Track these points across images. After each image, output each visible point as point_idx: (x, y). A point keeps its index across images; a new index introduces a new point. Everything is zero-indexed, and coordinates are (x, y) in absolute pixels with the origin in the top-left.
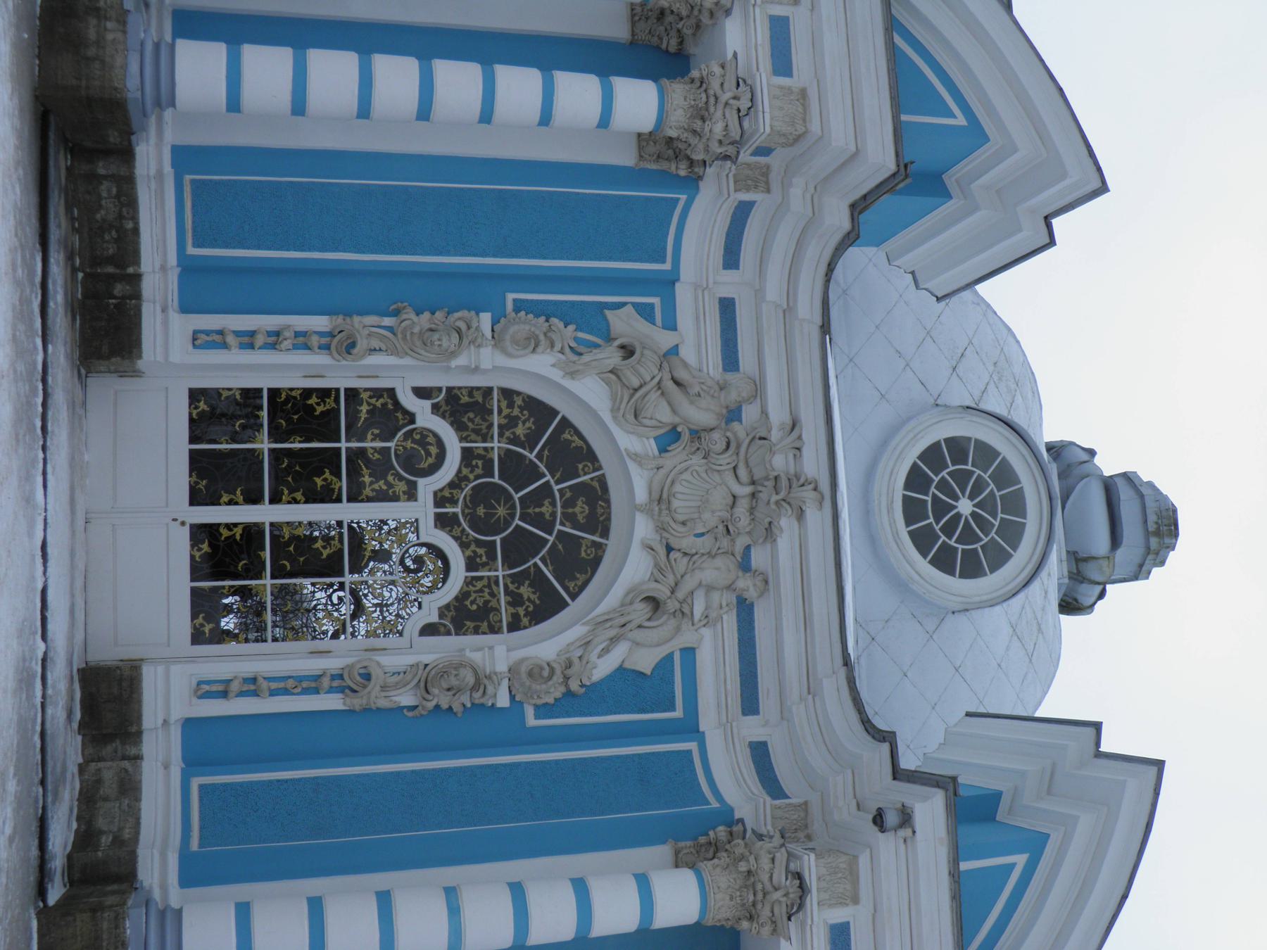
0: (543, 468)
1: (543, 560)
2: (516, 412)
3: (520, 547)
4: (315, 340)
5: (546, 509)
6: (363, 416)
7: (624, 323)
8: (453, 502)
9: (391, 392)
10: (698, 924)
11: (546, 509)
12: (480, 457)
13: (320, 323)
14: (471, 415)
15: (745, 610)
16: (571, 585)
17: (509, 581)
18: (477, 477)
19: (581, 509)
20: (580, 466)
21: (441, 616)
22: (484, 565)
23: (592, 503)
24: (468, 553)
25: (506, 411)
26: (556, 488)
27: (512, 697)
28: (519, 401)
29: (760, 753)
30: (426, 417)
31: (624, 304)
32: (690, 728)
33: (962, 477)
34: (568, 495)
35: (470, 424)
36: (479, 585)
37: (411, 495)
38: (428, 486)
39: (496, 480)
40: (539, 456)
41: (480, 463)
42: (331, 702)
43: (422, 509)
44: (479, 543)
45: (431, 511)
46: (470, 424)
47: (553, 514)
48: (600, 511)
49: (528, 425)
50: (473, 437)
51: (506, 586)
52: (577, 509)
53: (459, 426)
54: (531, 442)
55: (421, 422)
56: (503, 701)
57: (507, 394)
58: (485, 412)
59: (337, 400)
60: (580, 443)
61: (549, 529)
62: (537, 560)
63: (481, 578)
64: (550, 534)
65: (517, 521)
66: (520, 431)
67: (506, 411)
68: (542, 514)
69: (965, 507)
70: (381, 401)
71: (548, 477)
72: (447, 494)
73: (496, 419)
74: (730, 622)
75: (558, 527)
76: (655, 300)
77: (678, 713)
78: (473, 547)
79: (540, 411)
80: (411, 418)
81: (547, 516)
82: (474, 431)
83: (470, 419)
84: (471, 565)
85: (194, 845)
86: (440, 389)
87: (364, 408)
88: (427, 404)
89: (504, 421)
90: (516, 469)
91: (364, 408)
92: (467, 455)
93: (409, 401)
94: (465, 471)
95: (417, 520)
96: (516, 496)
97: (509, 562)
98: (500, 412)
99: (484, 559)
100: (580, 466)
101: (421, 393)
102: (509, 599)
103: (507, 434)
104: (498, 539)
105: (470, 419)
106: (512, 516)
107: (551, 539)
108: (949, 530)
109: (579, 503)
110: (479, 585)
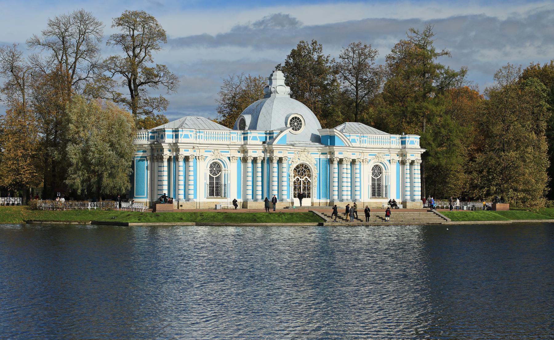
3: (305, 172)
7: (290, 163)
13: (290, 187)
15: (312, 153)
19: (301, 166)
29: (322, 154)
33: (296, 127)
37: (301, 181)
38: (300, 179)
42: (316, 188)
43: (302, 180)
54: (296, 170)
69: (296, 124)
74: (312, 155)
77: (318, 160)
79: (295, 169)
84: (305, 176)
108: (298, 126)
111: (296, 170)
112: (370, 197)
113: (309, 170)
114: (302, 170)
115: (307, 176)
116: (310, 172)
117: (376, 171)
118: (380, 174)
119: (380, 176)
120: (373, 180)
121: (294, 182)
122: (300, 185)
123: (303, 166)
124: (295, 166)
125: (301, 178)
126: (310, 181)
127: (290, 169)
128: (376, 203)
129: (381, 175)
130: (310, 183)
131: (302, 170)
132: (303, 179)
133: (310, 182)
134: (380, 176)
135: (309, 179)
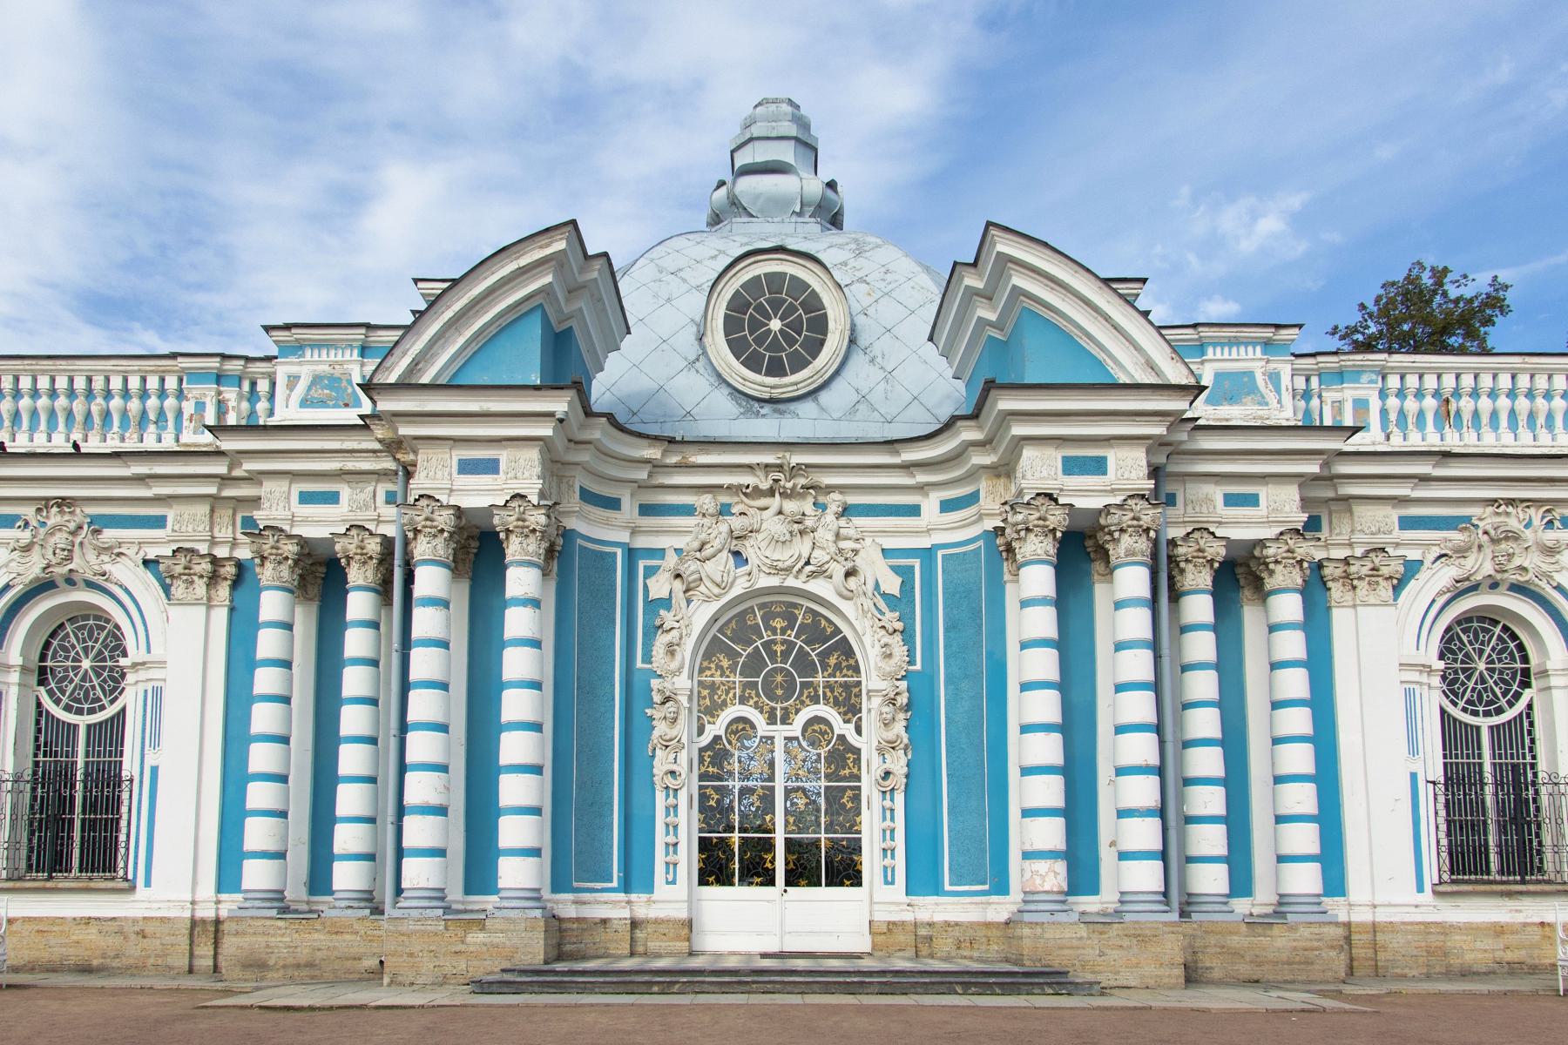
0: (750, 650)
1: (813, 650)
2: (713, 666)
4: (671, 800)
5: (779, 648)
6: (715, 770)
8: (773, 709)
9: (701, 750)
10: (1055, 567)
11: (779, 648)
12: (744, 691)
14: (716, 697)
16: (829, 630)
17: (826, 674)
18: (758, 695)
19: (778, 623)
20: (749, 623)
21: (847, 721)
22: (816, 691)
23: (774, 616)
24: (808, 702)
25: (713, 671)
26: (766, 638)
27: (904, 677)
28: (705, 664)
30: (717, 728)
31: (646, 586)
32: (927, 554)
34: (769, 633)
35: (723, 697)
36: (829, 694)
39: (760, 680)
40: (745, 651)
41: (748, 691)
42: (900, 798)
43: (780, 732)
44: (801, 693)
45: (779, 727)
46: (723, 697)
47: (784, 642)
48: (778, 609)
49: (721, 658)
50: (731, 695)
51: (830, 676)
52: (778, 626)
53: (724, 704)
54: (732, 655)
55: (722, 732)
56: (903, 685)
57: (701, 671)
58: (713, 687)
59: (707, 787)
60: (734, 622)
61: (791, 645)
62: (813, 654)
63: (824, 693)
64: (796, 644)
65: (787, 666)
66: (725, 663)
67: (713, 671)
68: (782, 651)
70: (706, 758)
71: (758, 643)
72: (767, 716)
73: (717, 679)
75: (792, 639)
76: (641, 564)
78: (804, 698)
80: (717, 739)
81: (783, 648)
82: (727, 695)
83: (719, 698)
85: (986, 887)
86: (699, 717)
87: (710, 769)
88: (708, 727)
89: (719, 673)
90: (754, 665)
91: (710, 769)
92: (743, 701)
93: (705, 740)
94: (751, 702)
95: (785, 738)
96: (771, 666)
97: (814, 672)
98: (712, 676)
99: (811, 690)
100: (749, 623)
101: (701, 731)
102: (838, 674)
103: (728, 673)
104: (798, 680)
105: (719, 698)
106: (782, 669)
107: (799, 643)
109: (774, 624)
110: (829, 694)
111: (732, 655)
112: (1431, 875)
113: (845, 649)
114: (785, 655)
115: (836, 704)
116: (857, 670)
117: (1482, 666)
118: (1526, 684)
119: (1521, 705)
120: (1455, 736)
121: (715, 754)
122: (771, 778)
123: (791, 619)
124: (701, 615)
125: (772, 720)
126: (853, 738)
127: (662, 640)
128: (1499, 930)
129: (1527, 694)
130: (857, 761)
131: (785, 655)
132: (796, 728)
133: (857, 751)
134: (1521, 705)
135: (841, 727)
